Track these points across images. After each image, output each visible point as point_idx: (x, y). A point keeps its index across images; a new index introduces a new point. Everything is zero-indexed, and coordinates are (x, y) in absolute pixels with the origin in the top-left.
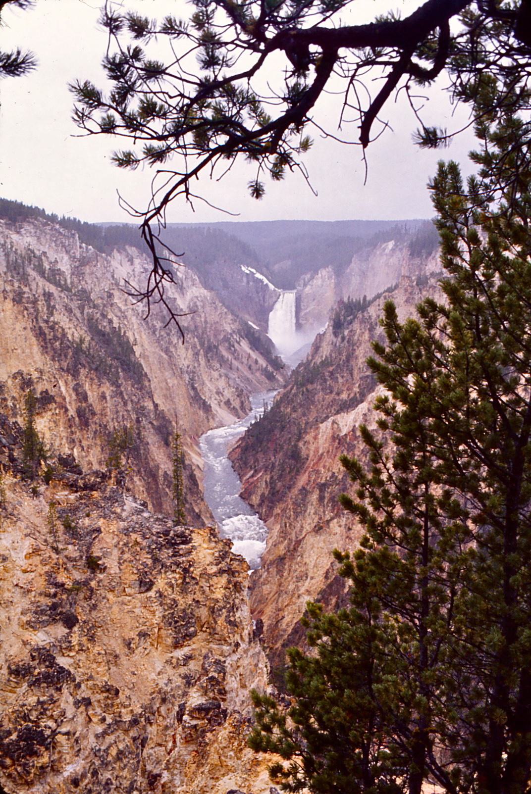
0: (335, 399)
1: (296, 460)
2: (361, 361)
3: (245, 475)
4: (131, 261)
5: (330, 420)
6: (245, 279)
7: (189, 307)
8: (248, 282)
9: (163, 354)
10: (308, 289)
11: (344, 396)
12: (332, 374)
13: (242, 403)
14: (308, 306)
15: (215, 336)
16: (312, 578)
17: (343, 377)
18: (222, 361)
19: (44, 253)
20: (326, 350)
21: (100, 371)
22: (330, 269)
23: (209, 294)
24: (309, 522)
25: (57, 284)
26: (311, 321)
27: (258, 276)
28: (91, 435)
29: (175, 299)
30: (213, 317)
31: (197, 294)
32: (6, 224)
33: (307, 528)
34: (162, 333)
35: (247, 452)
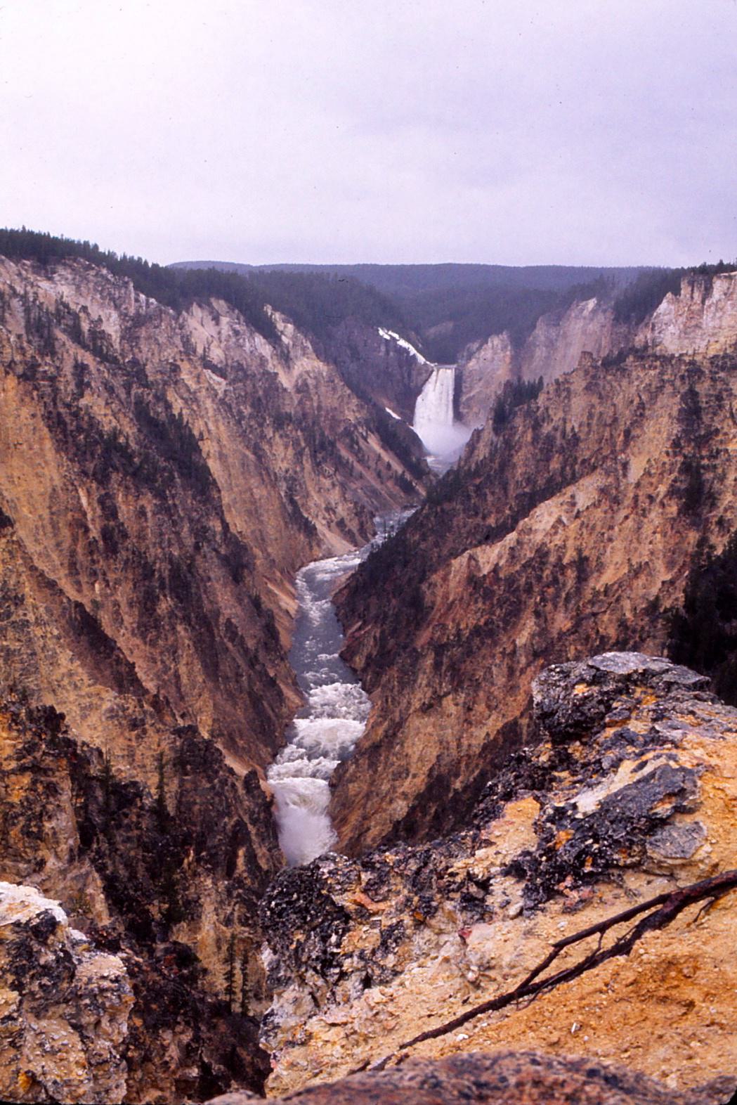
1: (417, 610)
2: (520, 471)
3: (350, 626)
4: (216, 319)
5: (466, 554)
6: (383, 348)
7: (296, 385)
8: (387, 352)
9: (248, 453)
11: (491, 521)
12: (478, 488)
13: (362, 525)
14: (472, 388)
15: (332, 428)
16: (414, 776)
17: (493, 493)
18: (340, 464)
19: (84, 309)
20: (482, 452)
21: (142, 477)
22: (505, 336)
23: (325, 368)
24: (420, 696)
25: (97, 352)
26: (475, 409)
27: (403, 343)
28: (120, 566)
29: (276, 374)
30: (330, 401)
31: (309, 368)
32: (33, 267)
33: (417, 704)
34: (252, 423)
35: (355, 596)
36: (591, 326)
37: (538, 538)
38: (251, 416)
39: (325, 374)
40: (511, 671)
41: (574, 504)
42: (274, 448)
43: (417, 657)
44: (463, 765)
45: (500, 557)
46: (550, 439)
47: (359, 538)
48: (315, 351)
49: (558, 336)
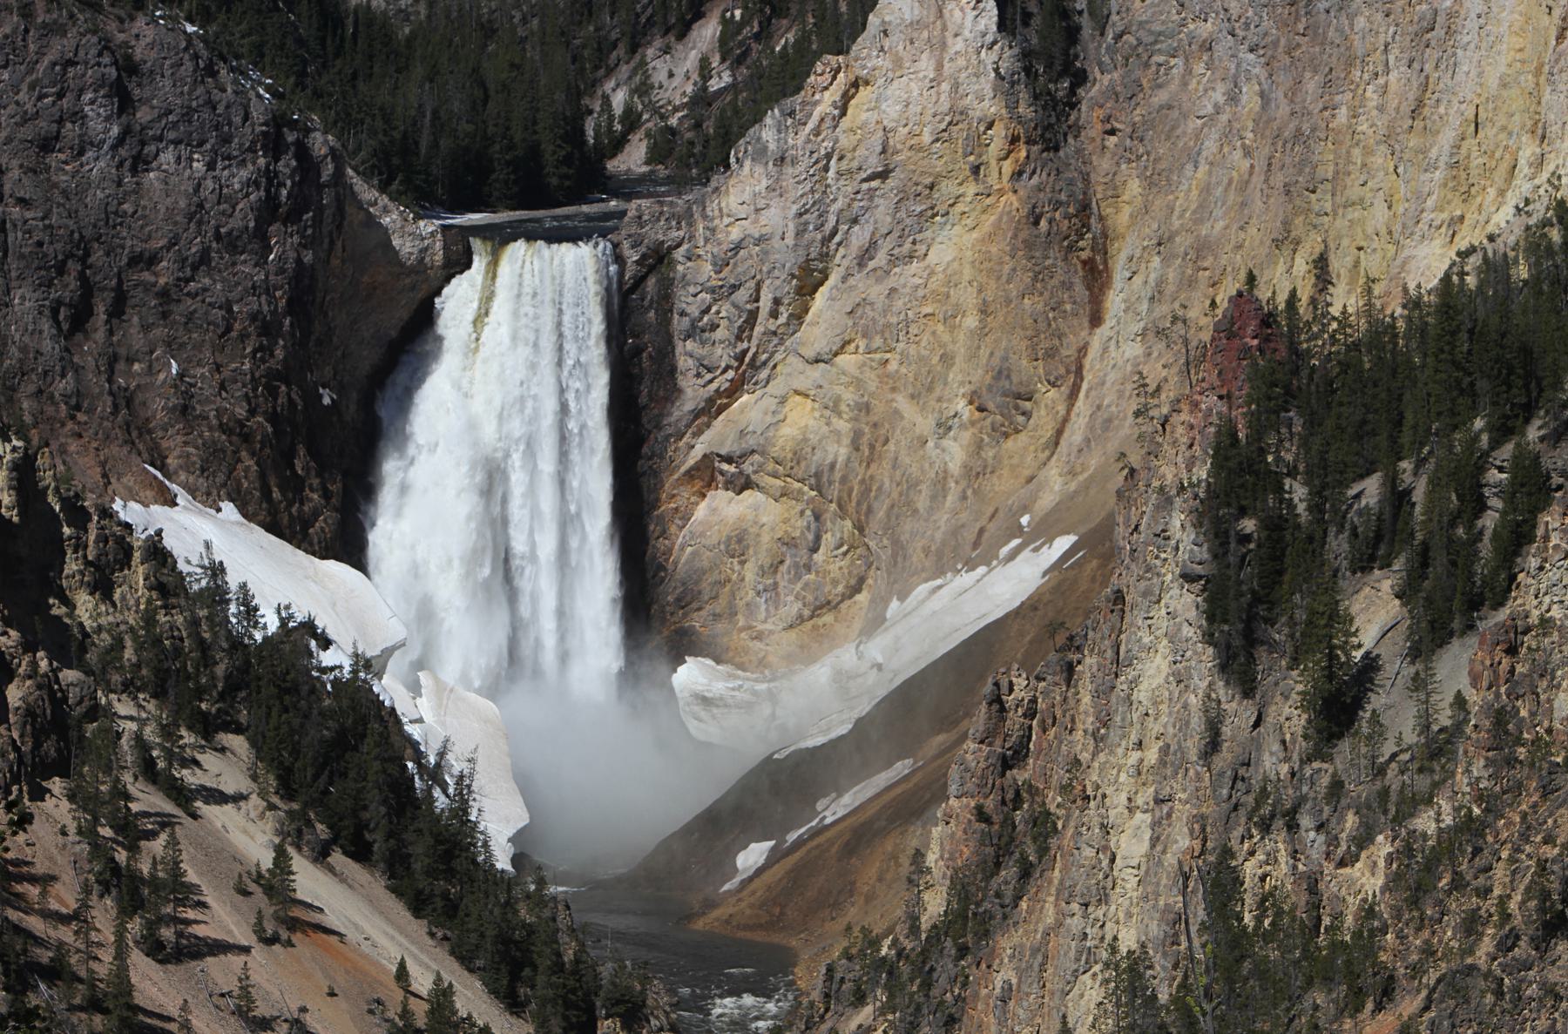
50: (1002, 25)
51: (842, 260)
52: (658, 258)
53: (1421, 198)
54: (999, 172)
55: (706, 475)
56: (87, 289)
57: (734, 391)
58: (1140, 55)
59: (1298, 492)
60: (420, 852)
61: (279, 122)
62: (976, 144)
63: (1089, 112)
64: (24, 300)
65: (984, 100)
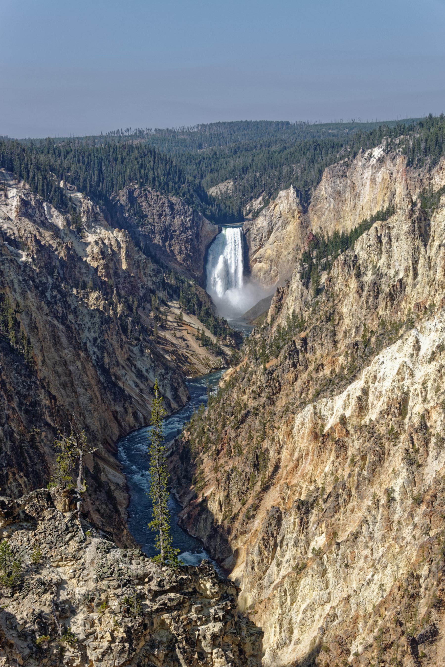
0: (312, 379)
5: (309, 408)
6: (168, 211)
9: (56, 322)
10: (262, 222)
16: (298, 642)
36: (379, 174)
37: (386, 385)
38: (56, 287)
39: (119, 239)
40: (389, 521)
41: (418, 349)
42: (80, 317)
43: (277, 518)
44: (360, 625)
45: (345, 407)
46: (376, 288)
47: (174, 405)
48: (106, 218)
49: (345, 187)
50: (297, 196)
51: (275, 230)
52: (248, 230)
53: (355, 219)
54: (297, 216)
55: (255, 261)
56: (167, 236)
57: (259, 248)
58: (317, 200)
59: (314, 261)
60: (202, 313)
61: (194, 211)
62: (293, 213)
63: (310, 208)
64: (158, 237)
65: (294, 207)
